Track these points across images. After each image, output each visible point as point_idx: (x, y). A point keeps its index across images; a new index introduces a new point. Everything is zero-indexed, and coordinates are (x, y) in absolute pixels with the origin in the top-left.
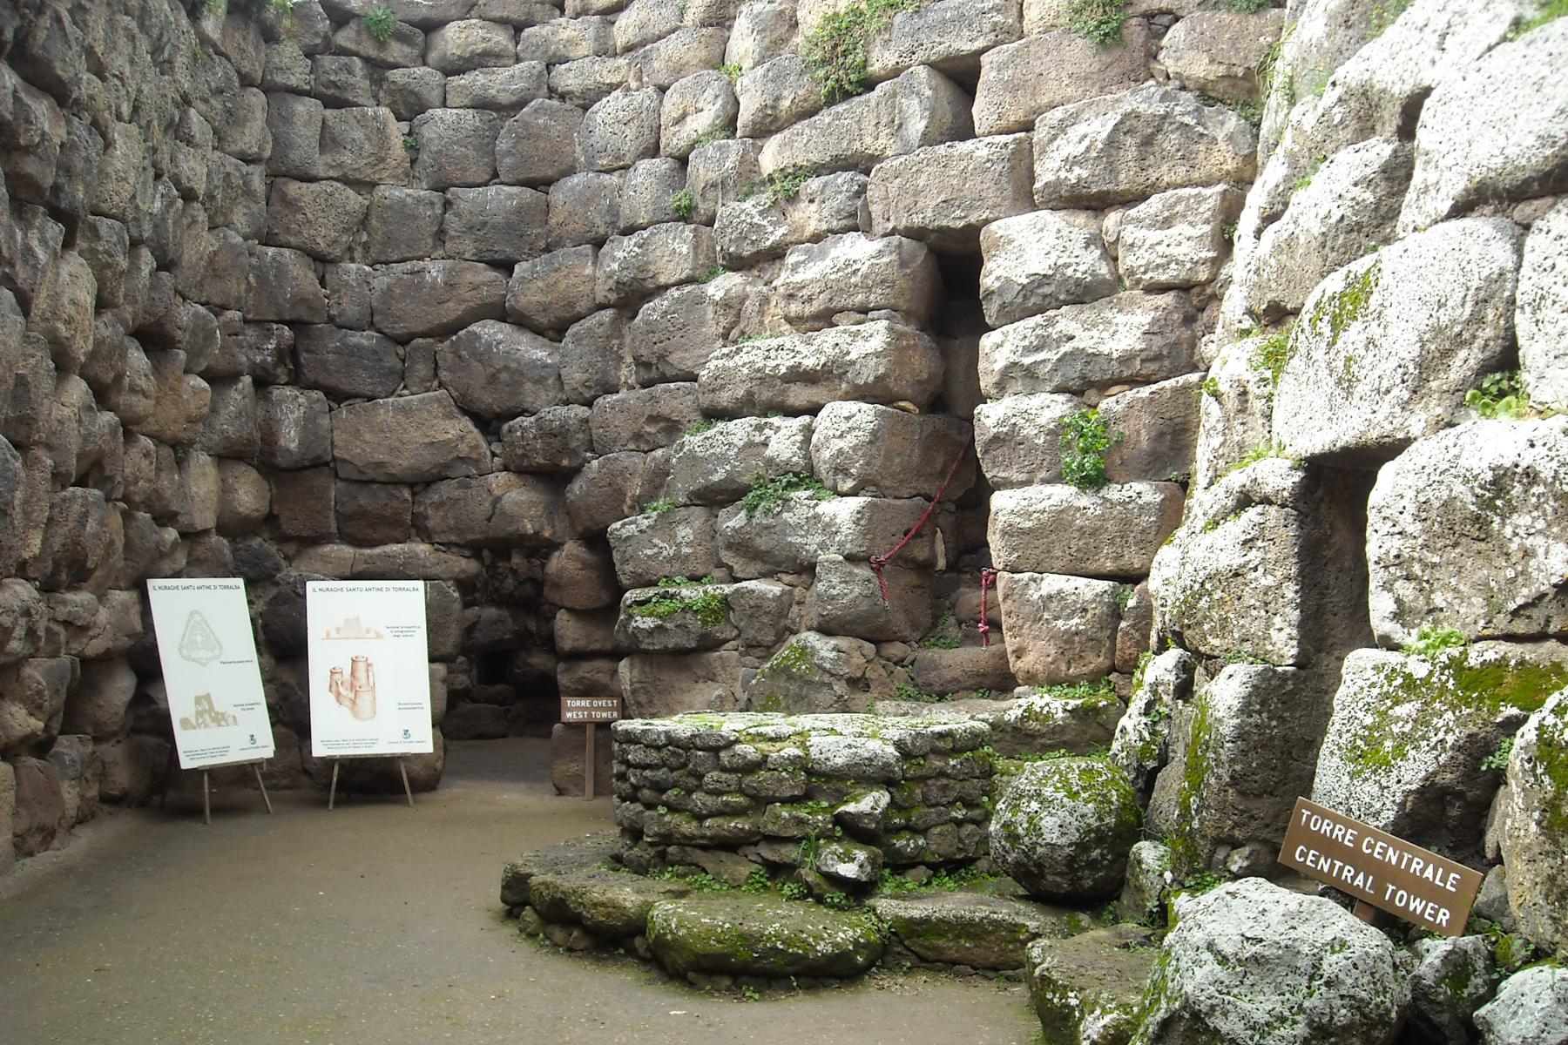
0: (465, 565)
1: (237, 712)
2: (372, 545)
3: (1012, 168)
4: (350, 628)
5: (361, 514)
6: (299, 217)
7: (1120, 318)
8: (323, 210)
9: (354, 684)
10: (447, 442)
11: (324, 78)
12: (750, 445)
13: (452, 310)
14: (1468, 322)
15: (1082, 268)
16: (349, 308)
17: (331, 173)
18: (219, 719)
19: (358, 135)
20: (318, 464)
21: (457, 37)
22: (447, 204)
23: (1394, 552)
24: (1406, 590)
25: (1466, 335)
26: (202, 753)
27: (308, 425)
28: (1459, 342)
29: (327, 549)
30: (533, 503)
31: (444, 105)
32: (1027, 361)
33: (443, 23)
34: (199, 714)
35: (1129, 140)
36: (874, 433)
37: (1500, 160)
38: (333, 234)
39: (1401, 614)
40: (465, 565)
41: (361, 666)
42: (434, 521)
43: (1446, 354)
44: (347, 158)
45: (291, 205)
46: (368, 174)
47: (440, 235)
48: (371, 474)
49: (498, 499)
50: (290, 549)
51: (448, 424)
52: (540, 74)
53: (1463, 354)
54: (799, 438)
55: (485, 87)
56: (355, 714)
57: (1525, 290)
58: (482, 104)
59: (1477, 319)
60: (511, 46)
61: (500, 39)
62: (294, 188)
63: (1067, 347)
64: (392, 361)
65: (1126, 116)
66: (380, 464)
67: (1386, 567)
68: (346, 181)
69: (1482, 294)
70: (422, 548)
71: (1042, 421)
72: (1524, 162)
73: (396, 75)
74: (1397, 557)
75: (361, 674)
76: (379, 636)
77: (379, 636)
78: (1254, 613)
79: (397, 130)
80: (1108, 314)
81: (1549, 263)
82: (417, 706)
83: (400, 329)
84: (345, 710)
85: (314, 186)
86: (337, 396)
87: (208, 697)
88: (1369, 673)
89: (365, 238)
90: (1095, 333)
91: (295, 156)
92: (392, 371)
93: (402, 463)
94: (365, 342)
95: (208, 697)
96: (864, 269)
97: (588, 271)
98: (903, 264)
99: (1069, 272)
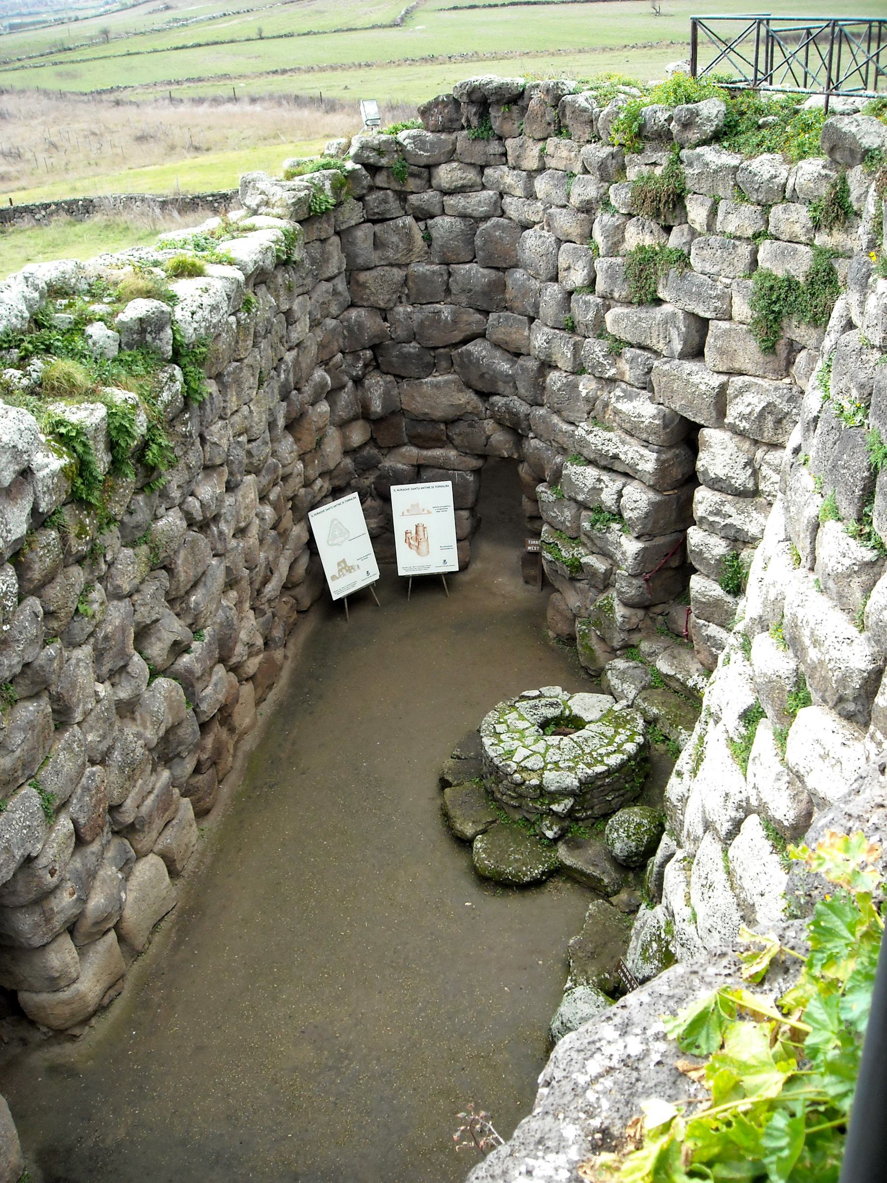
0: (475, 463)
1: (359, 562)
2: (428, 448)
3: (717, 403)
4: (414, 510)
5: (419, 436)
6: (368, 291)
7: (754, 514)
8: (379, 283)
9: (417, 538)
10: (460, 405)
11: (371, 212)
12: (594, 488)
13: (458, 336)
15: (739, 482)
16: (401, 333)
17: (382, 263)
18: (350, 569)
19: (395, 239)
20: (393, 413)
21: (446, 175)
22: (450, 274)
26: (341, 591)
27: (386, 397)
29: (404, 449)
30: (508, 442)
31: (443, 213)
32: (711, 519)
33: (438, 165)
34: (340, 571)
35: (770, 417)
36: (647, 513)
38: (388, 297)
40: (475, 463)
41: (421, 529)
42: (457, 441)
44: (390, 254)
45: (363, 286)
46: (404, 260)
47: (448, 291)
48: (422, 417)
49: (488, 437)
50: (385, 451)
51: (460, 395)
52: (496, 202)
54: (615, 497)
55: (464, 207)
56: (419, 553)
58: (464, 216)
60: (478, 180)
61: (471, 175)
62: (363, 277)
63: (728, 521)
64: (428, 359)
65: (769, 404)
66: (426, 414)
68: (391, 265)
70: (452, 453)
71: (714, 552)
73: (412, 198)
75: (421, 533)
76: (429, 512)
77: (429, 512)
79: (417, 230)
80: (750, 508)
82: (449, 547)
83: (431, 344)
84: (413, 552)
85: (374, 273)
86: (399, 377)
87: (344, 561)
89: (406, 291)
90: (742, 517)
91: (360, 261)
92: (428, 363)
93: (438, 414)
94: (412, 350)
95: (344, 561)
96: (646, 423)
97: (526, 333)
98: (665, 426)
99: (733, 481)
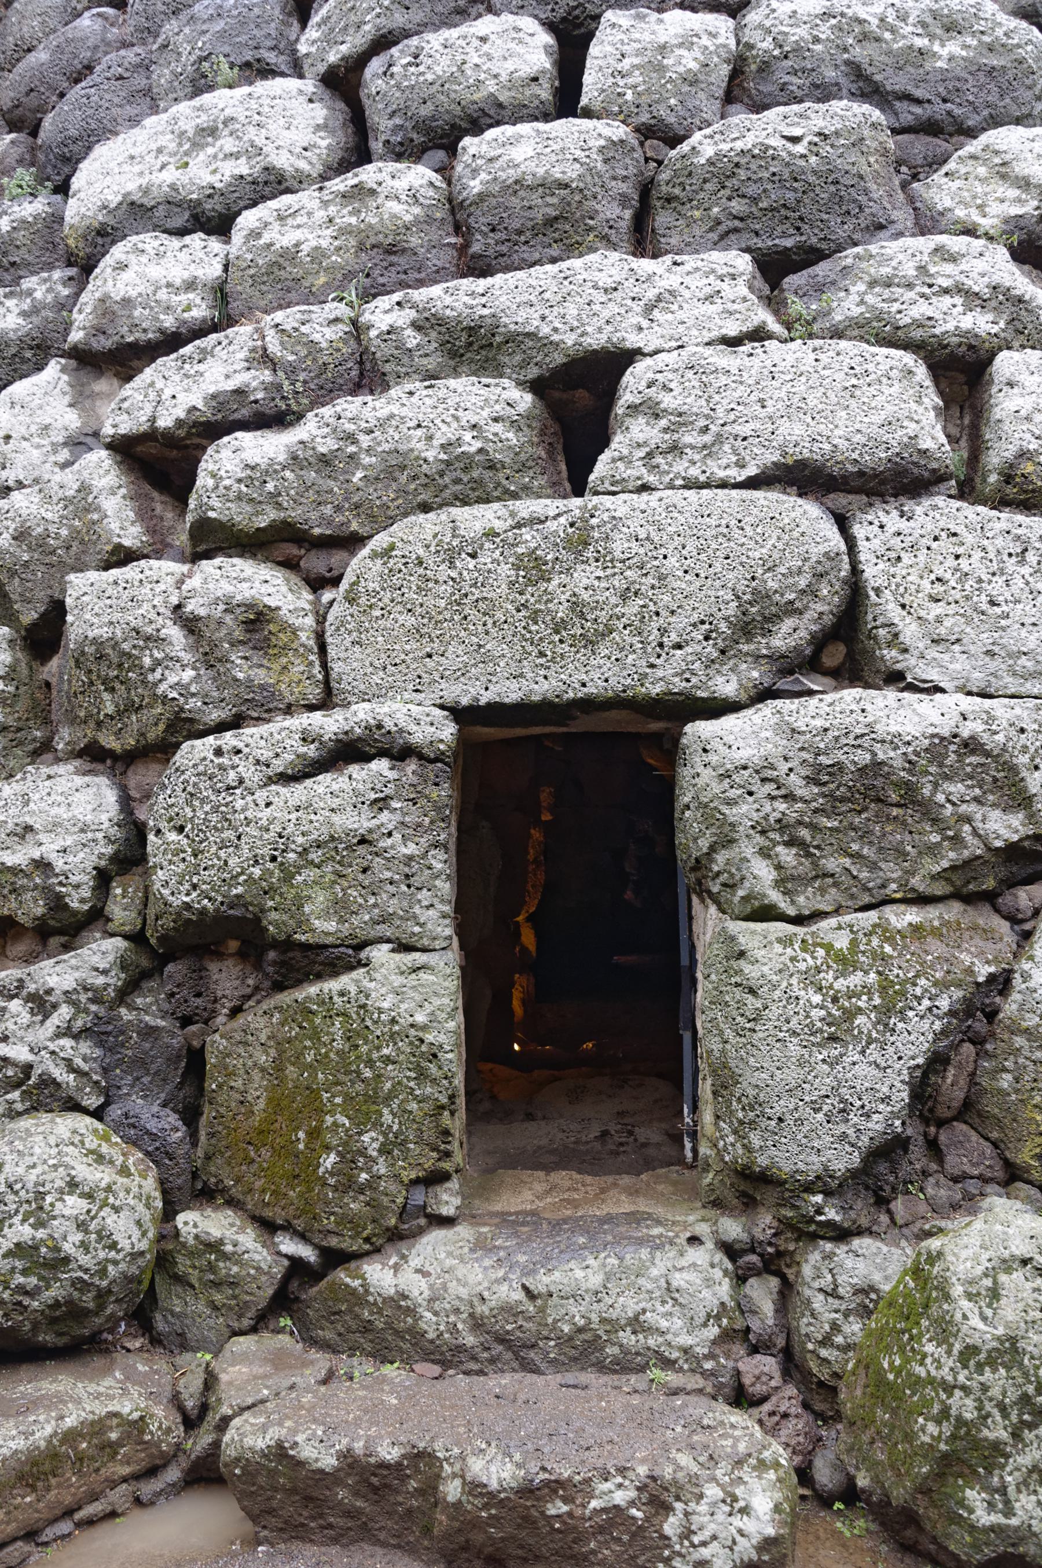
14: (803, 592)
23: (777, 815)
24: (787, 855)
25: (798, 605)
28: (791, 610)
37: (827, 447)
39: (785, 882)
43: (775, 618)
53: (788, 623)
57: (873, 572)
59: (811, 592)
67: (763, 832)
69: (820, 568)
72: (855, 456)
74: (779, 821)
78: (392, 889)
81: (893, 555)
88: (778, 948)
